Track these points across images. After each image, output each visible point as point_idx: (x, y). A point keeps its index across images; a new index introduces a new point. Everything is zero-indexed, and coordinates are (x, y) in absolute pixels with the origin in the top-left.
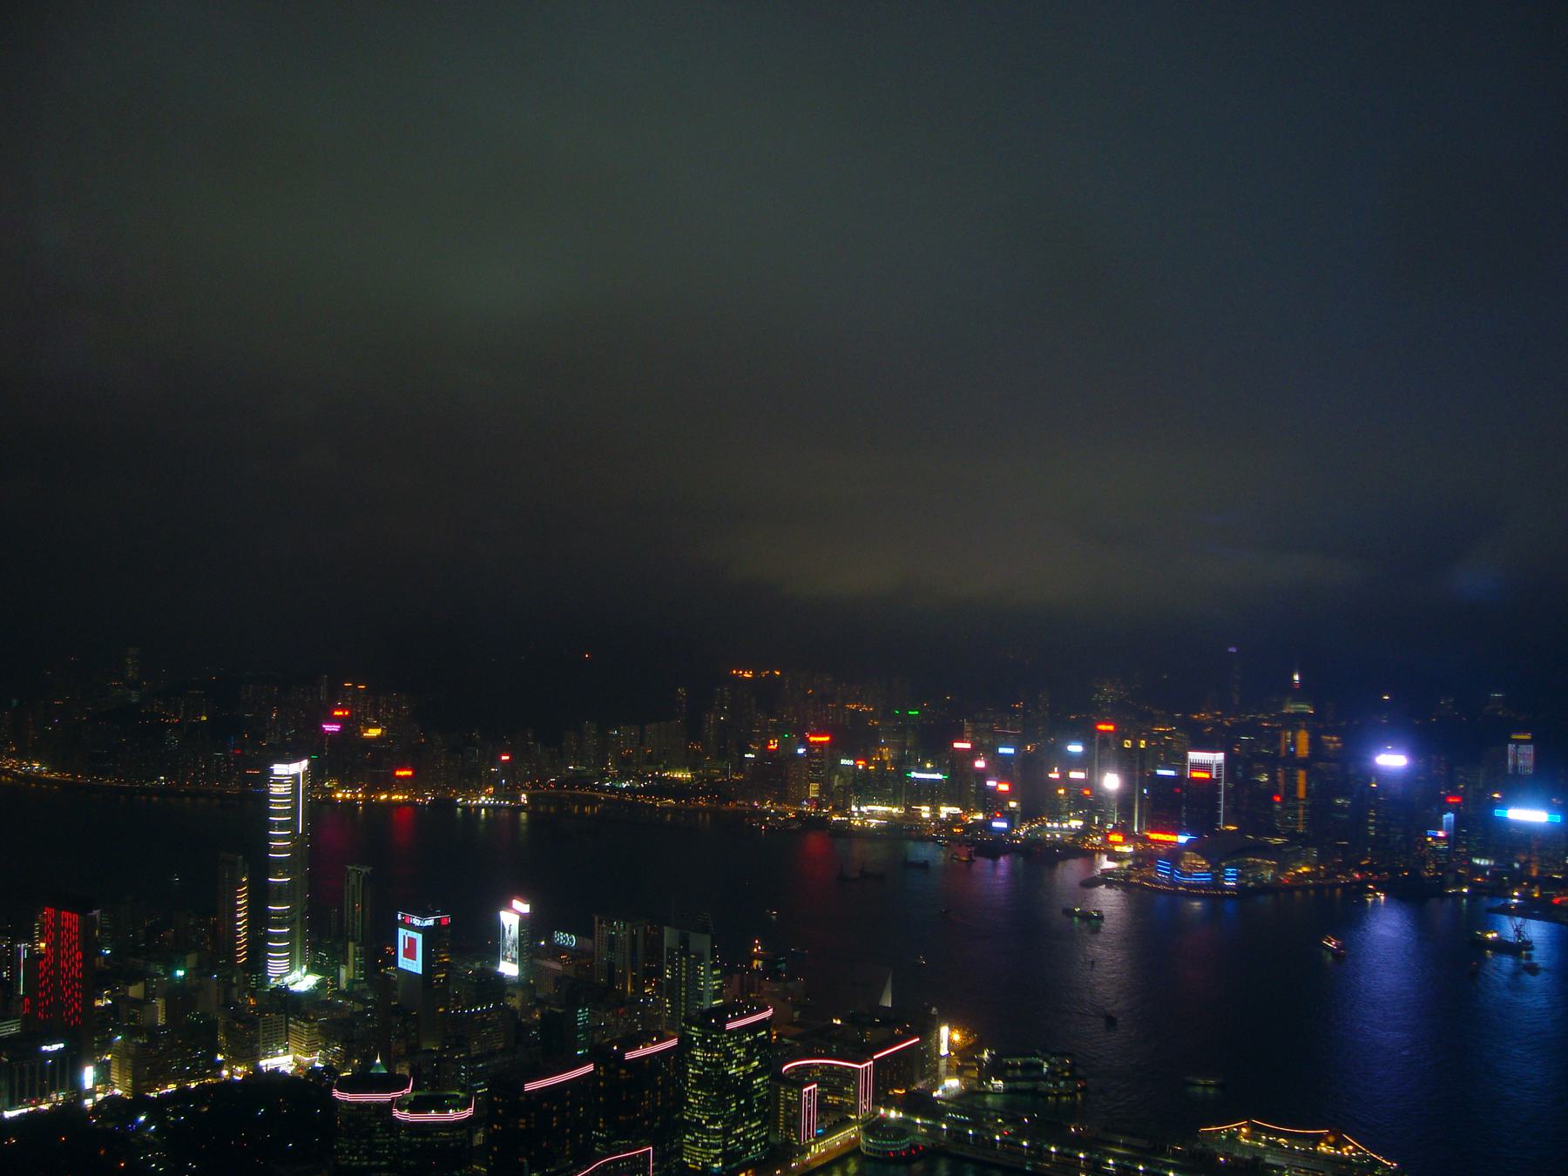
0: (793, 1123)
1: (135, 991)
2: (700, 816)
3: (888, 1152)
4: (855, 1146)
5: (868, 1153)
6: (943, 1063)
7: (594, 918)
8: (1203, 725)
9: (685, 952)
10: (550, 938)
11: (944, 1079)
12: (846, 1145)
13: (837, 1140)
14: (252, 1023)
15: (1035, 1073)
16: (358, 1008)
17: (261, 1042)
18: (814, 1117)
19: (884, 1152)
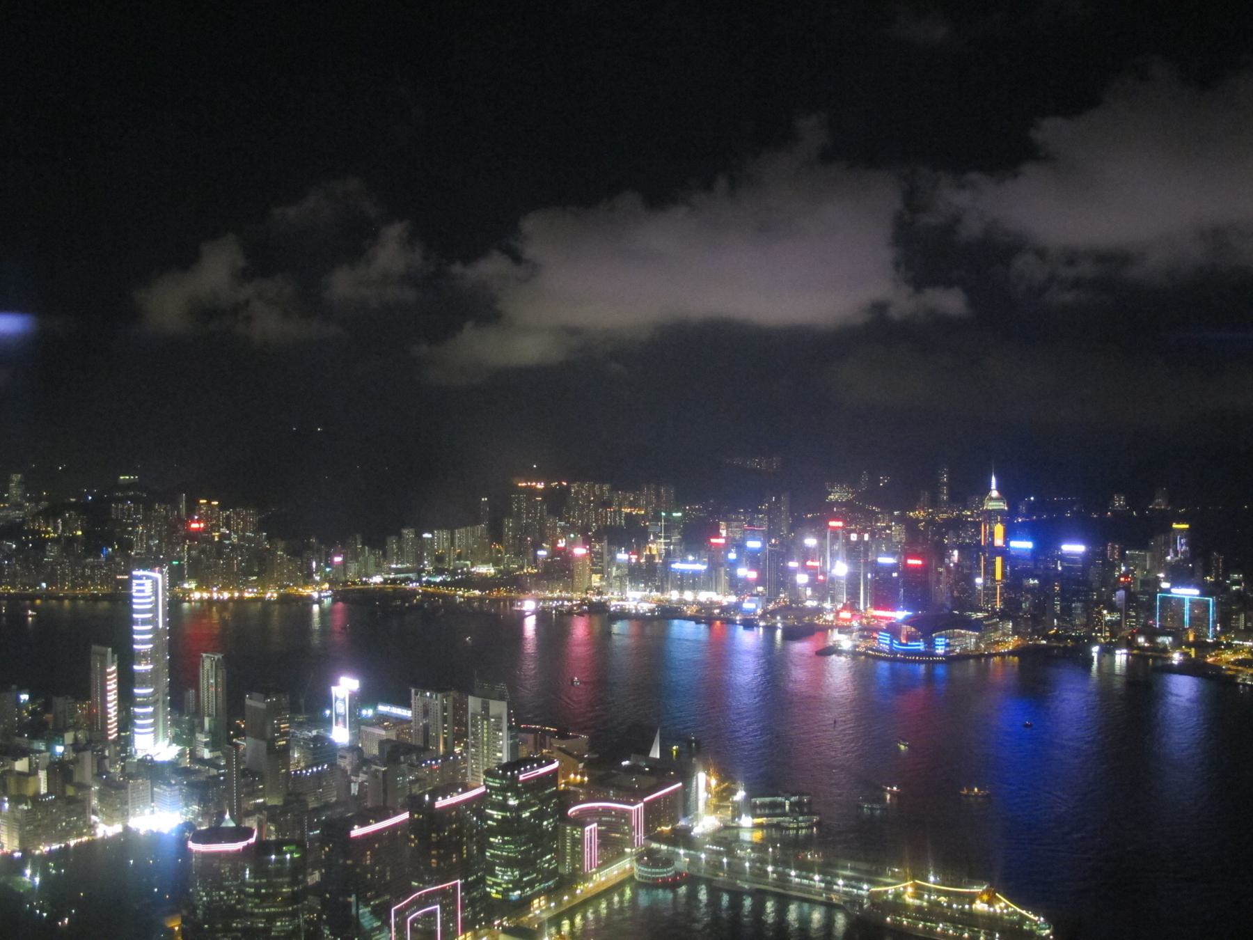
0: (578, 856)
1: (21, 765)
2: (502, 603)
3: (658, 879)
4: (630, 874)
5: (641, 880)
7: (410, 691)
8: (917, 521)
9: (486, 717)
10: (375, 708)
11: (703, 817)
12: (622, 873)
13: (614, 872)
14: (121, 787)
15: (778, 811)
16: (213, 772)
17: (130, 801)
18: (595, 852)
19: (653, 879)
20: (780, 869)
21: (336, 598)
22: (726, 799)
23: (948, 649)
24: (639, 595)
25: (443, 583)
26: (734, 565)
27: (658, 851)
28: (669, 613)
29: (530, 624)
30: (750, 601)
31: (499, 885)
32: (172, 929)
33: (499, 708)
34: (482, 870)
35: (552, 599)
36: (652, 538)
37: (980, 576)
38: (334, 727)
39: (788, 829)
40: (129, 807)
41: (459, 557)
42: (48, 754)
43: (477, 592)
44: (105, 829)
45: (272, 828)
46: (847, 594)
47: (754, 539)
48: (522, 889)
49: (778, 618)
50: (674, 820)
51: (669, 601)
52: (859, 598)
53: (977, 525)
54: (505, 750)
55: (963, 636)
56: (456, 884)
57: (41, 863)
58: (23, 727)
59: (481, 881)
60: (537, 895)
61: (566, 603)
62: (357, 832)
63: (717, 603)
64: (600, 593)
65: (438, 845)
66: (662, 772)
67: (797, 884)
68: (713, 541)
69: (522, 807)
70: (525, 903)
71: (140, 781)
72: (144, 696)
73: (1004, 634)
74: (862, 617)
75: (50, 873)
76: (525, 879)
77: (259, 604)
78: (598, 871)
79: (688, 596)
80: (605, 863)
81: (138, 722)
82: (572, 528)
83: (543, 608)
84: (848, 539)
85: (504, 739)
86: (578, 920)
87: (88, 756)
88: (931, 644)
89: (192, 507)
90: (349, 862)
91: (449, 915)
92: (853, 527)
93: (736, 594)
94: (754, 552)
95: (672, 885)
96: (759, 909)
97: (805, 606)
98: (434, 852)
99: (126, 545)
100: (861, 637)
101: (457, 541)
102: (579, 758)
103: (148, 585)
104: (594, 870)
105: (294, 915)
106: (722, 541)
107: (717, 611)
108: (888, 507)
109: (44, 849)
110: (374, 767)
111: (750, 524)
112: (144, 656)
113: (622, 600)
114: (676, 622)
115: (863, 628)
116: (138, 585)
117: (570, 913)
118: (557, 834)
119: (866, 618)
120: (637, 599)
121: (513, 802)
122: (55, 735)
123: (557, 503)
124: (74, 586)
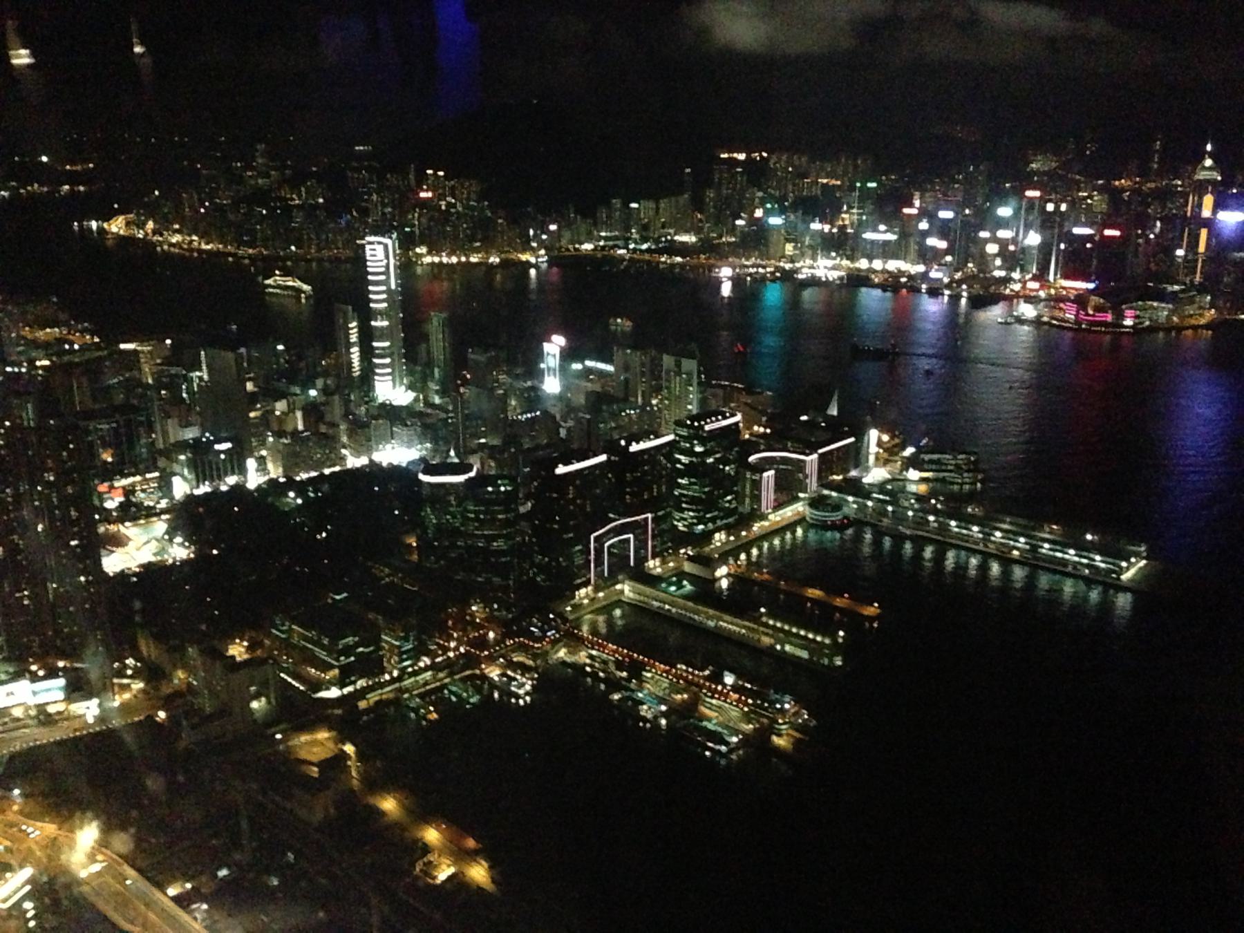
0: (757, 498)
1: (280, 407)
2: (701, 270)
5: (811, 521)
6: (872, 459)
9: (679, 373)
12: (795, 515)
13: (789, 512)
14: (366, 425)
16: (443, 415)
18: (772, 496)
20: (941, 519)
21: (551, 263)
22: (897, 454)
23: (1137, 321)
24: (830, 263)
25: (649, 250)
26: (925, 234)
27: (829, 497)
28: (857, 280)
29: (726, 290)
30: (937, 270)
31: (685, 519)
32: (410, 545)
33: (690, 365)
34: (671, 507)
35: (747, 267)
36: (845, 208)
37: (1181, 247)
38: (547, 378)
39: (953, 483)
40: (373, 443)
41: (663, 227)
42: (302, 397)
43: (679, 259)
44: (354, 462)
45: (493, 464)
46: (1038, 264)
47: (947, 209)
48: (705, 524)
49: (964, 287)
50: (845, 471)
51: (859, 270)
52: (1049, 269)
53: (1185, 196)
54: (695, 402)
55: (1155, 309)
56: (647, 518)
57: (301, 488)
58: (281, 374)
59: (668, 516)
60: (718, 530)
61: (761, 270)
62: (561, 470)
63: (904, 272)
64: (792, 261)
65: (630, 484)
66: (835, 430)
67: (957, 533)
68: (906, 211)
69: (707, 454)
70: (707, 536)
71: (381, 421)
72: (383, 348)
73: (1200, 308)
74: (1049, 287)
75: (309, 496)
76: (708, 516)
77: (484, 268)
78: (774, 512)
79: (877, 264)
80: (778, 506)
81: (378, 371)
82: (772, 199)
83: (738, 274)
84: (1044, 207)
85: (693, 394)
86: (755, 552)
87: (336, 398)
88: (1120, 316)
89: (421, 179)
90: (555, 495)
91: (640, 545)
92: (1053, 197)
93: (925, 264)
94: (946, 222)
95: (840, 527)
96: (918, 551)
97: (994, 277)
98: (628, 490)
99: (365, 212)
100: (1046, 307)
101: (661, 211)
102: (763, 413)
103: (380, 249)
104: (770, 511)
105: (507, 537)
106: (914, 211)
107: (904, 280)
108: (1091, 175)
109: (304, 476)
110: (581, 415)
111: (945, 195)
112: (381, 313)
113: (814, 268)
114: (864, 290)
115: (1049, 298)
116: (371, 250)
117: (746, 548)
118: (737, 479)
119: (1056, 288)
120: (827, 268)
121: (698, 449)
122: (308, 384)
123: (756, 174)
124: (319, 250)
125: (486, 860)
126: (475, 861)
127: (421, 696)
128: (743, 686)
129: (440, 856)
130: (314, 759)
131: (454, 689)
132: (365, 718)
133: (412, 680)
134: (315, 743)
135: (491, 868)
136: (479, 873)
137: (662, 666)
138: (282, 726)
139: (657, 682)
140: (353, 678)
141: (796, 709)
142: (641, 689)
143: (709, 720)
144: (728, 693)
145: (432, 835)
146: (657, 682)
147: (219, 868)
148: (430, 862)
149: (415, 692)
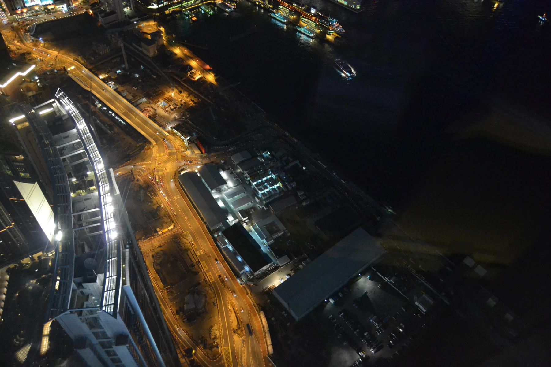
125: (213, 73)
126: (210, 73)
127: (190, 10)
128: (318, 14)
129: (196, 71)
130: (149, 32)
131: (203, 8)
132: (168, 18)
133: (187, 3)
134: (149, 26)
135: (215, 76)
136: (211, 78)
137: (287, 4)
138: (137, 19)
139: (284, 10)
140: (162, 1)
141: (338, 25)
142: (278, 12)
143: (303, 27)
144: (312, 17)
145: (193, 63)
146: (284, 10)
147: (118, 70)
148: (193, 73)
149: (187, 9)
